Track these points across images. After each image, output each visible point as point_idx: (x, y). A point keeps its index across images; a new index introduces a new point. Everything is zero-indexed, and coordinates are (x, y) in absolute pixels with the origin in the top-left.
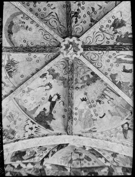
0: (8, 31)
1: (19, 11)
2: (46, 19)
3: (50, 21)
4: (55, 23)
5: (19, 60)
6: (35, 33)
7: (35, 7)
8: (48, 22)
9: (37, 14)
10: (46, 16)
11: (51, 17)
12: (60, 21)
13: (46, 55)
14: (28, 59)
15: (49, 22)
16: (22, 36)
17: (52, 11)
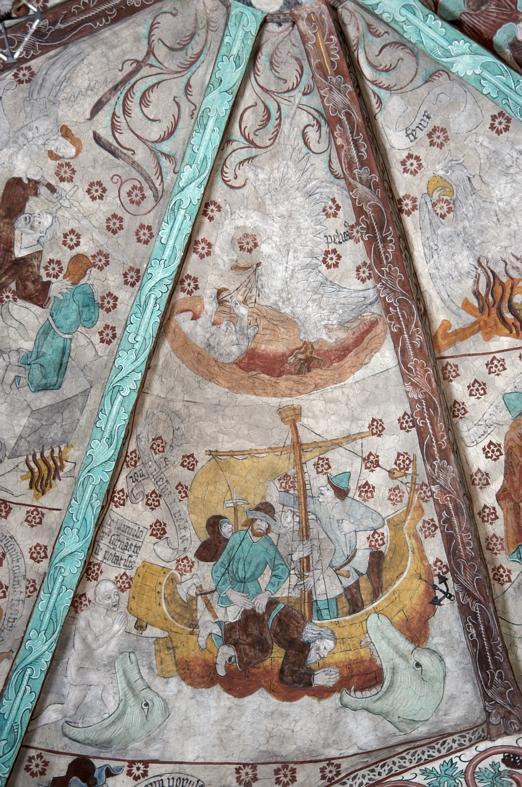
0: (299, 372)
1: (166, 347)
2: (151, 171)
3: (154, 132)
4: (153, 96)
5: (466, 262)
6: (260, 207)
7: (107, 256)
8: (166, 147)
9: (146, 235)
10: (135, 174)
11: (126, 138)
12: (128, 68)
13: (383, 93)
14: (442, 208)
15: (162, 140)
16: (303, 283)
17: (87, 139)
